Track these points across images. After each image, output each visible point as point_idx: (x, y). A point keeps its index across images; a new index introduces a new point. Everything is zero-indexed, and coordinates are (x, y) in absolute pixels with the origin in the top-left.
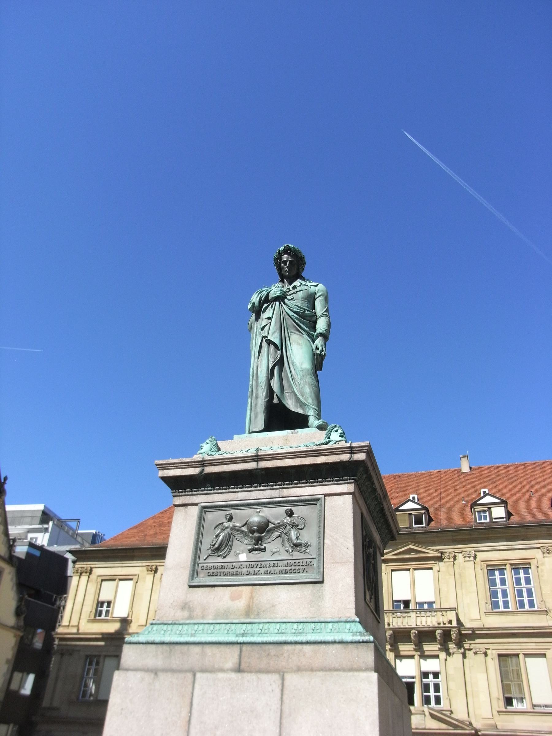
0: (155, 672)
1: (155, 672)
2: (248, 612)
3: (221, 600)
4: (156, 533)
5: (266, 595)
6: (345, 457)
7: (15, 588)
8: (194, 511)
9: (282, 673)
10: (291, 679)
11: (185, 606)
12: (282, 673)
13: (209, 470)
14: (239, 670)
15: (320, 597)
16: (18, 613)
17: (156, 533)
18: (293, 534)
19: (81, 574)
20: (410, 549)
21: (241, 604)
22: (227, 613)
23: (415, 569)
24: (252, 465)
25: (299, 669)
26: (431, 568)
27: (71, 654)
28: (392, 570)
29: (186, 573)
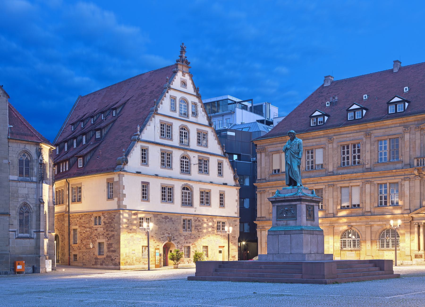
0: (273, 235)
1: (273, 235)
2: (286, 225)
3: (283, 223)
5: (289, 222)
7: (230, 168)
8: (276, 207)
9: (290, 235)
11: (276, 224)
12: (290, 235)
13: (277, 200)
14: (285, 234)
15: (296, 222)
16: (235, 179)
18: (292, 211)
21: (285, 223)
22: (283, 225)
24: (284, 199)
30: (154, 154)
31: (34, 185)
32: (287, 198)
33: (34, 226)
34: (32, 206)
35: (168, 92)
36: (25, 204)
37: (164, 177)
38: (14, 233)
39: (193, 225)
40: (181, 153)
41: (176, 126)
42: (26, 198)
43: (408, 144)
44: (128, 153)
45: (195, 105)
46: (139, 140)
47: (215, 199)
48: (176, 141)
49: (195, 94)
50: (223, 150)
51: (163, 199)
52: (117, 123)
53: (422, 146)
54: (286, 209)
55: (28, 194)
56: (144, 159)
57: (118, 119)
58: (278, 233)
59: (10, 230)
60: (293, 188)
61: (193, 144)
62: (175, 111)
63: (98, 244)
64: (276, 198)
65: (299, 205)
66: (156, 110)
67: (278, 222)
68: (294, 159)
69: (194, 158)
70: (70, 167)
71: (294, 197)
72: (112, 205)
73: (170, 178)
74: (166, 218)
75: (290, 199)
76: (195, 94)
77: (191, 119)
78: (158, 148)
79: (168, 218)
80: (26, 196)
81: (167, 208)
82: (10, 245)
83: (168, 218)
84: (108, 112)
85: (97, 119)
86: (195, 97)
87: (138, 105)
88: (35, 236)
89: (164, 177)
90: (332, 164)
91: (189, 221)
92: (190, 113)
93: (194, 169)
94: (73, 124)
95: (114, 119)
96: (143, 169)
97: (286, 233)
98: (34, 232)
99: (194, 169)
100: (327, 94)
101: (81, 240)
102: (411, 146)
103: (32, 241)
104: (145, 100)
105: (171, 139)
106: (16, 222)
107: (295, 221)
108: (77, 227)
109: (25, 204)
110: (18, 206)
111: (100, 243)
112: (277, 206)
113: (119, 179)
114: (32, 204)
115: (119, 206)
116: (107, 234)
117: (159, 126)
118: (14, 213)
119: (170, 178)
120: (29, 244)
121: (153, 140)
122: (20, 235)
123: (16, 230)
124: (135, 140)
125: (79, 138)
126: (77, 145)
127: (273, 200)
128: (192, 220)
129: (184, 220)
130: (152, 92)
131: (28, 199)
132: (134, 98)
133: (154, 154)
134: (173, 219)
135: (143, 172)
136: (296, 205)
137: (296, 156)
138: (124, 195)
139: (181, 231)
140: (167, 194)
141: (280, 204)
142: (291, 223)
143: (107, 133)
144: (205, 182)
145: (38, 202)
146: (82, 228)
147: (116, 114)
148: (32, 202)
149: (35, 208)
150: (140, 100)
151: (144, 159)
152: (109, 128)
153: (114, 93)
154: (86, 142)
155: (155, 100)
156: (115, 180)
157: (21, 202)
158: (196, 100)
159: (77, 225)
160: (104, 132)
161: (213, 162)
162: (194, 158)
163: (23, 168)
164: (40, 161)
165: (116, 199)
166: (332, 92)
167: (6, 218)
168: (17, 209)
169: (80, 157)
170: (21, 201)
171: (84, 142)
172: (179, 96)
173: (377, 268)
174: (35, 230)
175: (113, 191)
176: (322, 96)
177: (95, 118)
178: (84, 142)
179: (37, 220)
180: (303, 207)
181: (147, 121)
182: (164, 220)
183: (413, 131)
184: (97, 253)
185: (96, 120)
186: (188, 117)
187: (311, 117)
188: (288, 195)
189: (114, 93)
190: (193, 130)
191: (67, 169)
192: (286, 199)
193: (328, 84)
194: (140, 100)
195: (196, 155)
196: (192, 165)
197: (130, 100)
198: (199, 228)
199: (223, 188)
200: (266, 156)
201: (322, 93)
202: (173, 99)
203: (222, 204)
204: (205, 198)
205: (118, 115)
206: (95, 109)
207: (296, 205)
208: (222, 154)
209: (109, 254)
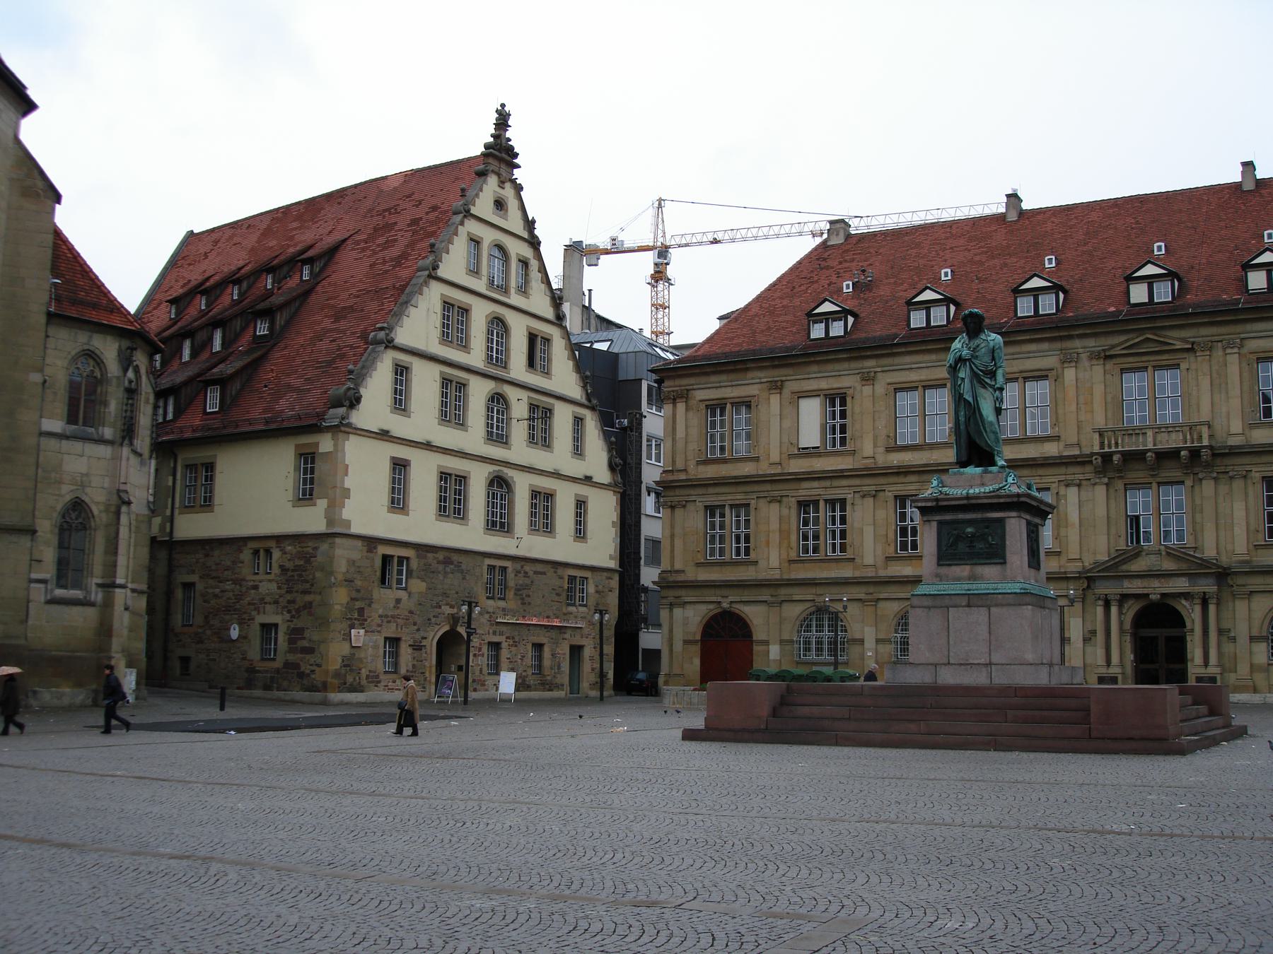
0: (929, 608)
1: (929, 608)
4: (769, 328)
6: (1015, 500)
8: (935, 524)
9: (989, 607)
10: (993, 610)
12: (989, 607)
13: (941, 503)
14: (969, 606)
16: (612, 467)
17: (769, 328)
19: (674, 399)
20: (1148, 339)
23: (1156, 368)
24: (965, 502)
25: (996, 605)
26: (1177, 366)
27: (684, 506)
28: (1123, 371)
29: (935, 560)
31: (104, 451)
32: (977, 498)
33: (98, 568)
34: (96, 512)
35: (462, 223)
36: (78, 505)
38: (42, 586)
39: (511, 583)
40: (487, 387)
41: (480, 312)
42: (83, 486)
43: (1071, 393)
45: (524, 263)
46: (390, 344)
48: (476, 357)
49: (526, 235)
50: (584, 387)
51: (442, 511)
52: (313, 298)
53: (1109, 399)
54: (969, 530)
55: (87, 475)
57: (319, 288)
58: (947, 601)
59: (34, 576)
60: (986, 472)
61: (518, 367)
63: (258, 628)
64: (937, 500)
65: (1013, 520)
66: (435, 268)
67: (944, 570)
68: (982, 391)
69: (519, 406)
70: (178, 412)
71: (999, 497)
72: (311, 520)
74: (447, 562)
75: (986, 501)
76: (526, 235)
77: (515, 299)
79: (452, 563)
82: (30, 622)
83: (452, 563)
84: (286, 269)
85: (249, 287)
86: (525, 245)
87: (375, 253)
88: (100, 596)
90: (871, 435)
92: (513, 284)
93: (519, 432)
94: (172, 302)
95: (307, 287)
96: (399, 425)
97: (972, 600)
98: (98, 585)
99: (519, 432)
100: (840, 263)
101: (206, 617)
102: (1082, 399)
103: (91, 613)
104: (396, 240)
106: (49, 555)
107: (999, 567)
108: (193, 578)
109: (78, 505)
110: (59, 507)
111: (264, 626)
112: (940, 523)
113: (335, 445)
114: (97, 503)
115: (330, 522)
116: (289, 602)
117: (438, 307)
118: (46, 528)
120: (81, 620)
121: (420, 345)
122: (59, 592)
123: (47, 576)
124: (380, 342)
125: (201, 336)
126: (194, 354)
127: (929, 504)
128: (510, 570)
130: (415, 222)
131: (88, 490)
132: (364, 237)
133: (426, 382)
134: (464, 567)
135: (396, 432)
136: (1001, 521)
137: (988, 381)
141: (948, 517)
142: (989, 571)
143: (288, 323)
144: (542, 473)
145: (115, 500)
146: (211, 582)
147: (311, 273)
148: (97, 497)
149: (104, 516)
150: (381, 240)
152: (293, 310)
153: (295, 225)
154: (223, 344)
155: (432, 241)
156: (321, 451)
157: (68, 498)
158: (527, 252)
159: (193, 572)
160: (280, 320)
161: (563, 417)
162: (519, 406)
163: (79, 400)
164: (126, 383)
165: (322, 504)
166: (853, 260)
167: (25, 541)
168: (55, 515)
169: (214, 382)
170: (67, 493)
171: (217, 345)
172: (488, 236)
173: (1203, 709)
174: (99, 581)
175: (312, 480)
176: (827, 268)
177: (245, 285)
178: (217, 345)
179: (106, 553)
180: (1016, 527)
181: (412, 294)
182: (441, 567)
183: (1085, 362)
184: (254, 653)
185: (246, 292)
186: (505, 290)
187: (810, 314)
188: (977, 491)
189: (295, 225)
190: (519, 329)
191: (170, 416)
192: (973, 501)
193: (838, 240)
194: (381, 240)
195: (524, 395)
196: (514, 422)
197: (349, 242)
198: (524, 593)
199: (583, 490)
200: (687, 410)
201: (825, 259)
202: (475, 242)
203: (580, 533)
205: (317, 278)
206: (241, 263)
207: (1001, 521)
208: (584, 401)
209: (291, 657)
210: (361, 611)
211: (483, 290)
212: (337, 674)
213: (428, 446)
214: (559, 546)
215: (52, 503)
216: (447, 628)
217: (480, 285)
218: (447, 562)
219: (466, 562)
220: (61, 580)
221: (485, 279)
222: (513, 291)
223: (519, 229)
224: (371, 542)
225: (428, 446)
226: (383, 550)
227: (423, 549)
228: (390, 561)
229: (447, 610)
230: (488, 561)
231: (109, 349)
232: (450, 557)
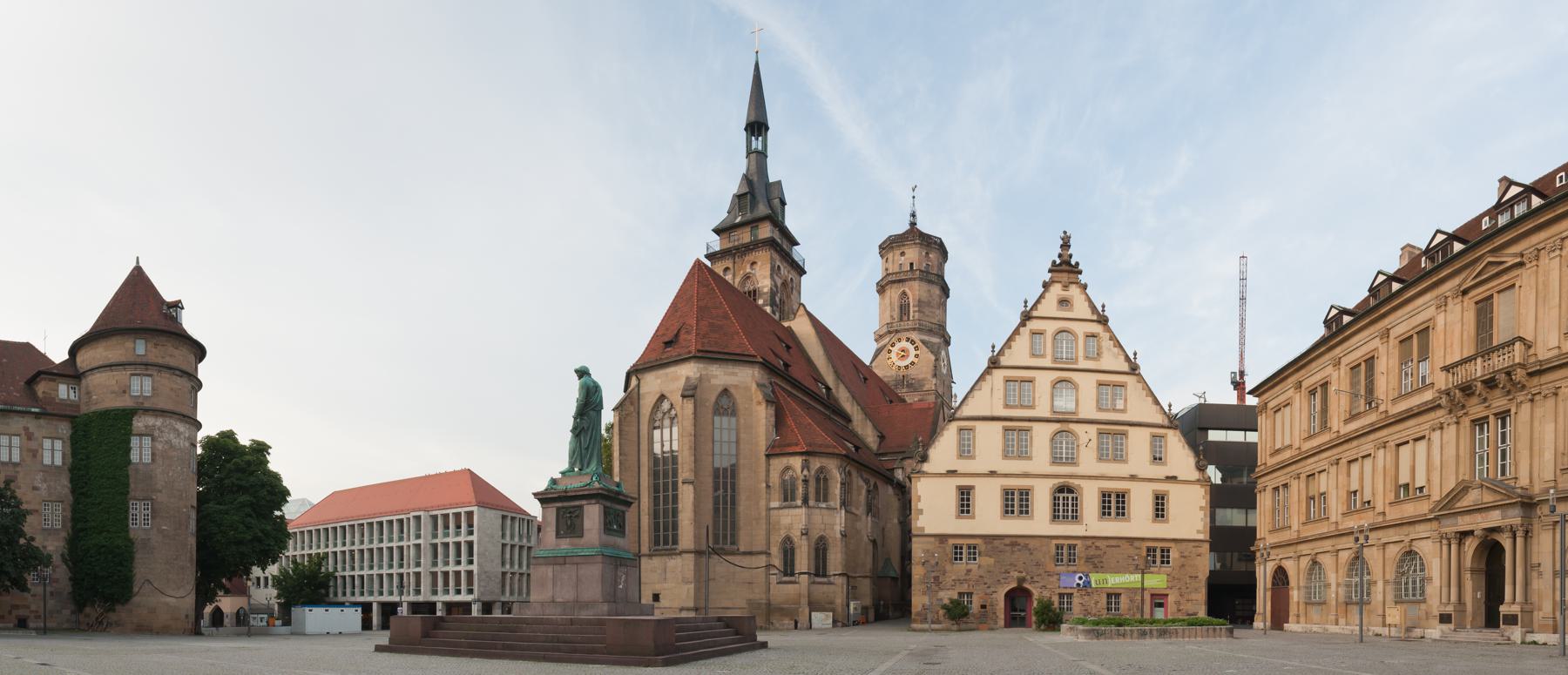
30: (989, 438)
36: (788, 539)
37: (1006, 475)
40: (1057, 426)
41: (1044, 380)
44: (928, 444)
46: (953, 419)
47: (1140, 501)
56: (965, 451)
62: (1043, 356)
73: (1026, 475)
74: (1013, 544)
78: (999, 425)
80: (790, 527)
81: (1113, 528)
89: (1006, 475)
91: (1072, 547)
105: (1032, 407)
119: (1026, 475)
121: (987, 413)
129: (1057, 547)
138: (921, 512)
139: (1051, 566)
140: (1017, 502)
151: (965, 451)
158: (1096, 328)
167: (763, 557)
170: (783, 533)
204: (1114, 504)
210: (936, 578)
211: (1049, 364)
212: (918, 614)
213: (993, 474)
214: (1139, 523)
215: (777, 539)
216: (1014, 585)
217: (1047, 362)
218: (1013, 544)
219: (1032, 544)
220: (817, 575)
221: (1049, 357)
222: (1081, 359)
223: (1089, 315)
224: (942, 538)
225: (993, 474)
226: (951, 541)
227: (989, 539)
228: (959, 548)
229: (1016, 574)
230: (1055, 541)
231: (797, 462)
232: (1015, 541)
